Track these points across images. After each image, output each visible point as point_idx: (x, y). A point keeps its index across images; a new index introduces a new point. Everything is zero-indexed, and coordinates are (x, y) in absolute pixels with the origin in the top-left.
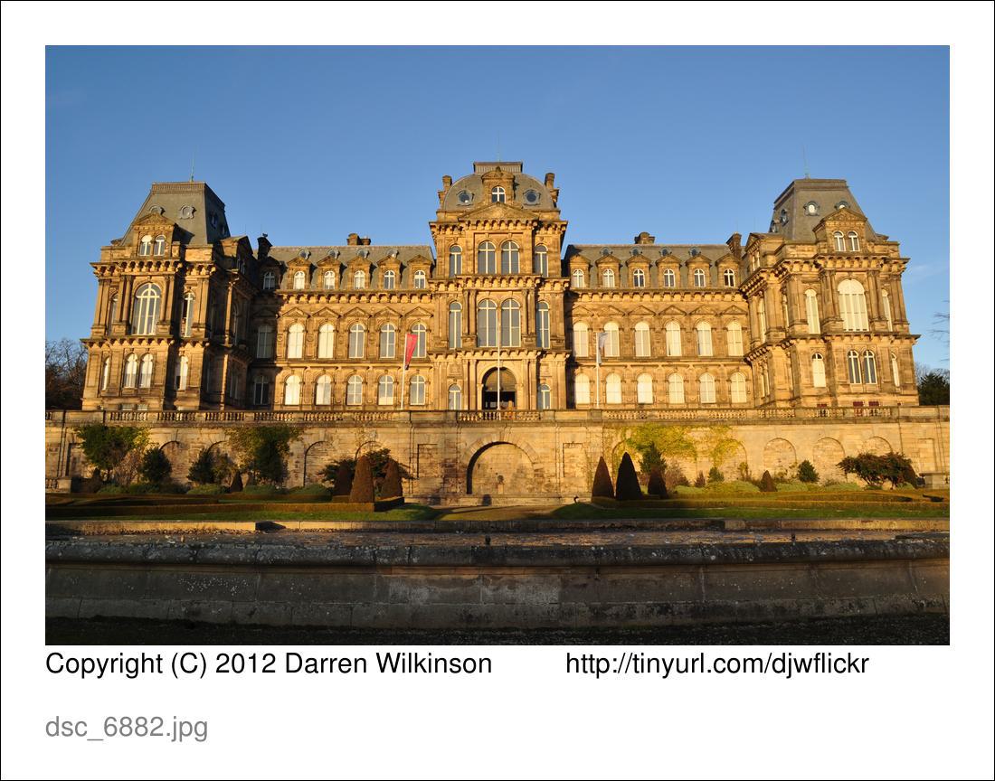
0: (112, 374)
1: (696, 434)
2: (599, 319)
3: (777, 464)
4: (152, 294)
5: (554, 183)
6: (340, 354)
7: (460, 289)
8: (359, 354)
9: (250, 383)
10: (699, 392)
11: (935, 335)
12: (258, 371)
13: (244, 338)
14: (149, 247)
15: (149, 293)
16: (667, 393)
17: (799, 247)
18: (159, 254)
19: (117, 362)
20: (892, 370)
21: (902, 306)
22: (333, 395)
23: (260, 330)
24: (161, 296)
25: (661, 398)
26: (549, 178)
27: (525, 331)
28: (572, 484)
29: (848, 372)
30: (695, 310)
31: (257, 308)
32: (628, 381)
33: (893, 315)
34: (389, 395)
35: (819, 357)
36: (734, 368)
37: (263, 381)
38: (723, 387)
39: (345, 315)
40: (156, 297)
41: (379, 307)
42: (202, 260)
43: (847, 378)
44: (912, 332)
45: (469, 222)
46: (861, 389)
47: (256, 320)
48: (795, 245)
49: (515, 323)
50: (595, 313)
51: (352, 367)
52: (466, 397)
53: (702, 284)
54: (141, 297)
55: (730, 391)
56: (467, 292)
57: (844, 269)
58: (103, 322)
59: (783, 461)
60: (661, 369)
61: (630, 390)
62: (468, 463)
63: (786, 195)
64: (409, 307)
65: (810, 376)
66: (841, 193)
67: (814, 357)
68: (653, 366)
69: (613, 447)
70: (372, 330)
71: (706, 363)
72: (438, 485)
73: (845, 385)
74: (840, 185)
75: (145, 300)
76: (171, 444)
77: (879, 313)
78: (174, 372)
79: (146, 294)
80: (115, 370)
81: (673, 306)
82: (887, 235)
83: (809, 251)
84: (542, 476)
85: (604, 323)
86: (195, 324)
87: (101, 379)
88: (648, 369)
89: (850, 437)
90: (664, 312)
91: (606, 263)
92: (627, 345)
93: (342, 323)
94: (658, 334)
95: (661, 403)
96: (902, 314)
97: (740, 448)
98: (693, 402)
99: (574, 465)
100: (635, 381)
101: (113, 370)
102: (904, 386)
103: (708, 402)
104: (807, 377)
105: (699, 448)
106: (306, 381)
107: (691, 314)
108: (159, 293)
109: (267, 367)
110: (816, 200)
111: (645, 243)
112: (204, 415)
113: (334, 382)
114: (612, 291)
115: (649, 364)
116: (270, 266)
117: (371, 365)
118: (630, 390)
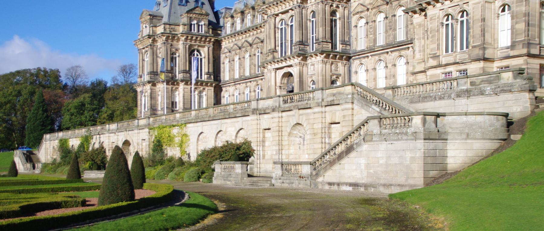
32: (390, 66)
51: (255, 81)
68: (405, 49)
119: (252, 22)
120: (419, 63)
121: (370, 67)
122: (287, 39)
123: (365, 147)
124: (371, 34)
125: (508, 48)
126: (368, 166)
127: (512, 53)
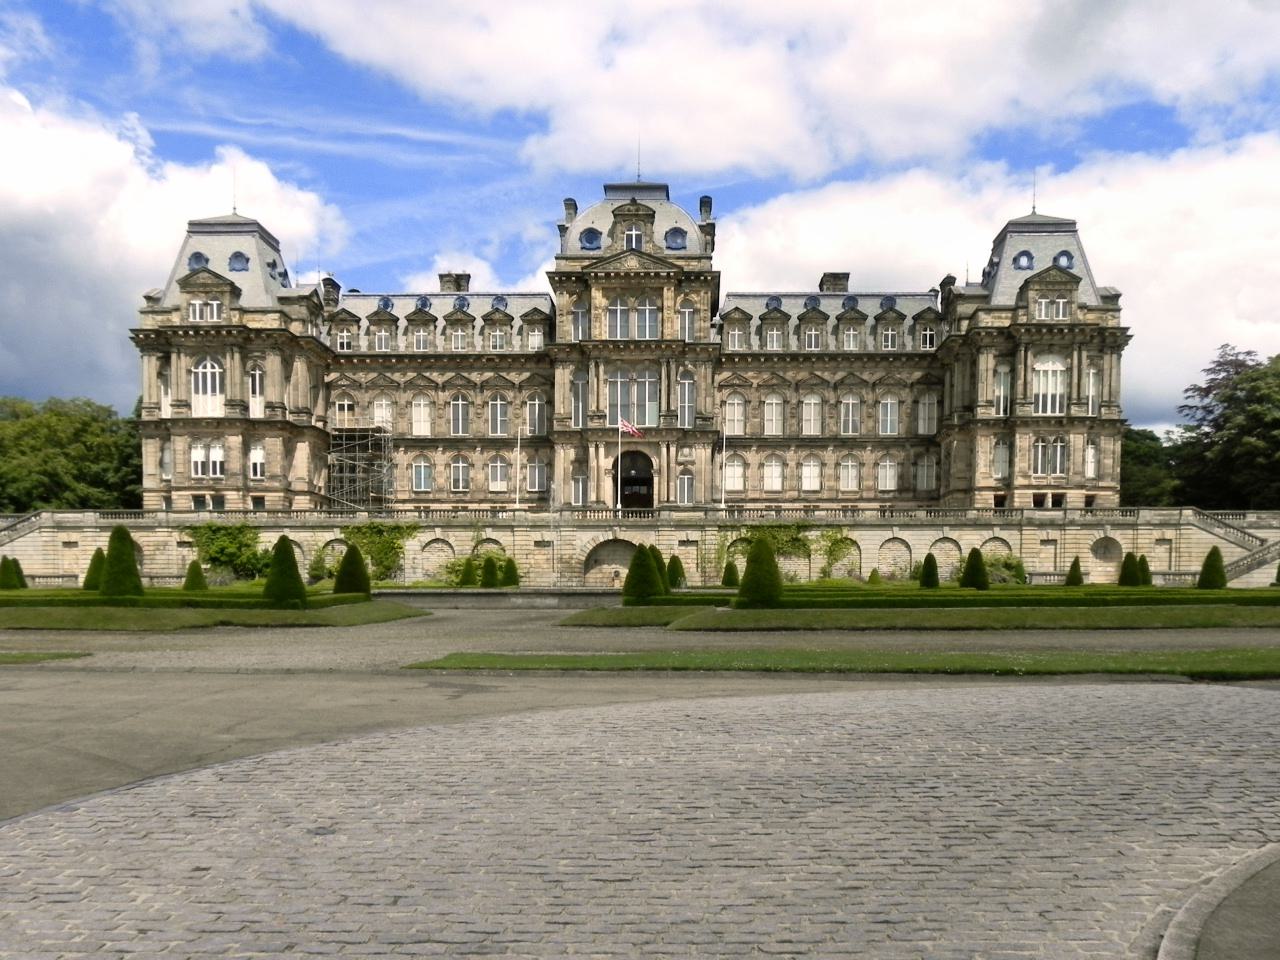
0: (178, 461)
1: (812, 532)
11: (1186, 411)
19: (181, 448)
29: (1032, 462)
43: (1029, 468)
45: (596, 274)
46: (1044, 482)
48: (989, 311)
57: (1044, 342)
61: (793, 478)
72: (555, 580)
78: (249, 459)
82: (1120, 289)
92: (794, 421)
99: (689, 561)
107: (874, 384)
122: (655, 405)
124: (755, 417)
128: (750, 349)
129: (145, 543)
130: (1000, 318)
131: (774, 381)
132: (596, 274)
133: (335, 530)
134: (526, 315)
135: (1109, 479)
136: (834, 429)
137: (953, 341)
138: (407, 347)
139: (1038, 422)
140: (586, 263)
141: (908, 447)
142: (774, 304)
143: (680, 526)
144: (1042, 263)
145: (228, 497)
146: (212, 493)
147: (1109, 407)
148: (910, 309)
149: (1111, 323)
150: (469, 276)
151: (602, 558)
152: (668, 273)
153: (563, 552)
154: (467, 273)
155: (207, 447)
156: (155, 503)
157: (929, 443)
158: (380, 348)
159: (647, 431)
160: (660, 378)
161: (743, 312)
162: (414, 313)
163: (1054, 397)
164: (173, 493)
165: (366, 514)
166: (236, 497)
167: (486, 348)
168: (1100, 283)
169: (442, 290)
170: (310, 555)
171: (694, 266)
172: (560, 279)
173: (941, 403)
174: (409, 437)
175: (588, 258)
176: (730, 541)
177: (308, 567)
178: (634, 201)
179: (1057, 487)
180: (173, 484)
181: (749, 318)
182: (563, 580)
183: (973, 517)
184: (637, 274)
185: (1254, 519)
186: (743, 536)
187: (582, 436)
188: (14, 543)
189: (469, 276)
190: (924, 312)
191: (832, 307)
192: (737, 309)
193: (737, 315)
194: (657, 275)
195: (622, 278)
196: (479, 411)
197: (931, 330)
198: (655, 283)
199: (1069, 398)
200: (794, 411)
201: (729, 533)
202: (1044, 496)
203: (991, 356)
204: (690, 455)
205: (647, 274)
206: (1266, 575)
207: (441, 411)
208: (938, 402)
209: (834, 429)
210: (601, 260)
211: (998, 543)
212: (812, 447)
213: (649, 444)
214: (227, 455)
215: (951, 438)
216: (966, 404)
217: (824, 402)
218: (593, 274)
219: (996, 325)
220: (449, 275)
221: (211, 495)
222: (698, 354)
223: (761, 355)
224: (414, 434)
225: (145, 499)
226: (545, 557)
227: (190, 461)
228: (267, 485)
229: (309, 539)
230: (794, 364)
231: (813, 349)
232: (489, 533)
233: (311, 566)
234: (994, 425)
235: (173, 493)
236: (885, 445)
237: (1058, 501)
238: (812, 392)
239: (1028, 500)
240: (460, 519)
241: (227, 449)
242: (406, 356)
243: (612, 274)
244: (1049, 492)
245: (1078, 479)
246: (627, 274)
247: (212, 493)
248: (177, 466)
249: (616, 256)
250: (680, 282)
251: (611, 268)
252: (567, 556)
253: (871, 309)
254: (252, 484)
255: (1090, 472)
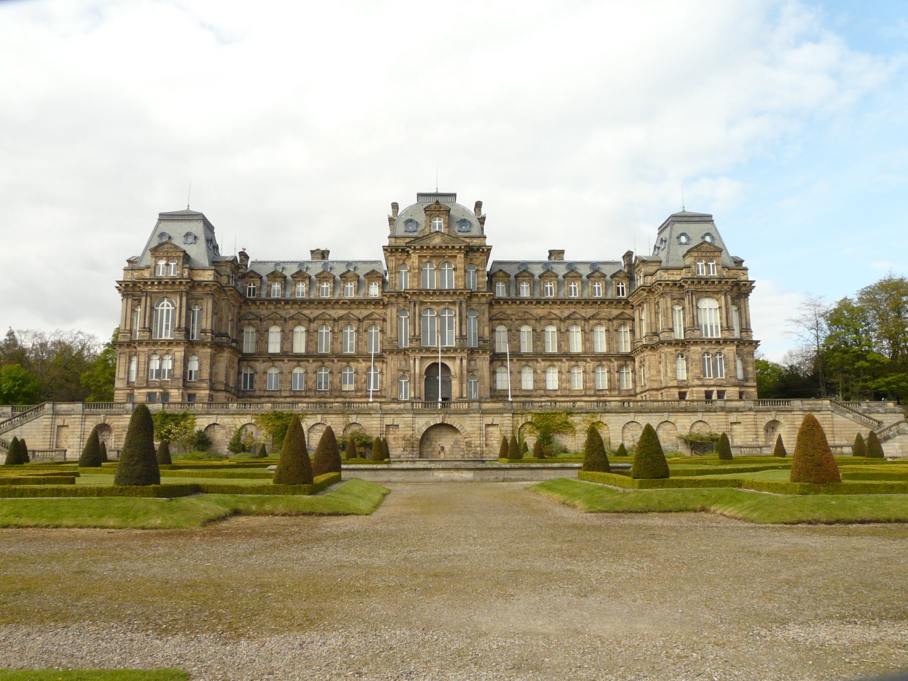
1: (576, 418)
2: (517, 322)
3: (631, 439)
4: (168, 306)
5: (482, 209)
6: (311, 349)
7: (407, 300)
8: (326, 349)
9: (239, 373)
10: (594, 381)
12: (245, 363)
13: (234, 338)
14: (163, 268)
15: (165, 305)
16: (569, 381)
17: (670, 272)
18: (172, 275)
20: (736, 368)
21: (748, 317)
22: (306, 382)
23: (246, 330)
24: (176, 308)
25: (564, 385)
26: (478, 205)
27: (458, 334)
28: (490, 452)
30: (593, 316)
31: (242, 312)
32: (539, 371)
33: (741, 325)
34: (351, 383)
35: (682, 357)
36: (622, 362)
37: (249, 372)
38: (614, 377)
39: (315, 319)
40: (171, 308)
41: (342, 312)
42: (206, 279)
44: (754, 338)
45: (415, 247)
47: (242, 322)
49: (450, 327)
50: (514, 317)
52: (412, 385)
53: (599, 294)
54: (160, 308)
55: (619, 380)
56: (413, 303)
58: (128, 328)
59: (635, 437)
60: (566, 364)
62: (420, 438)
63: (665, 225)
64: (365, 313)
65: (675, 371)
66: (705, 228)
67: (678, 357)
69: (519, 426)
70: (336, 330)
71: (600, 359)
72: (400, 453)
73: (699, 379)
74: (706, 219)
75: (162, 311)
76: (212, 427)
77: (727, 323)
78: (187, 367)
79: (163, 306)
80: (142, 367)
81: (575, 312)
82: (742, 258)
83: (677, 274)
84: (471, 447)
85: (521, 325)
86: (202, 330)
87: (128, 372)
88: (555, 363)
89: (681, 420)
90: (568, 317)
91: (523, 277)
92: (539, 343)
93: (312, 325)
94: (563, 335)
95: (565, 389)
96: (748, 323)
97: (606, 427)
98: (590, 389)
100: (544, 372)
101: (140, 366)
102: (746, 379)
103: (601, 388)
104: (671, 372)
105: (577, 428)
106: (284, 371)
107: (589, 319)
108: (173, 305)
109: (253, 360)
110: (687, 233)
111: (555, 258)
112: (236, 405)
113: (306, 372)
114: (527, 300)
115: (556, 358)
116: (252, 277)
117: (336, 360)
118: (540, 381)
119: (308, 293)
120: (671, 380)
121: (515, 370)
123: (898, 437)
125: (742, 380)
126: (901, 447)
127: (747, 384)
128: (509, 296)
129: (116, 426)
130: (673, 274)
131: (526, 317)
132: (415, 247)
133: (248, 416)
134: (367, 274)
135: (752, 381)
136: (566, 348)
137: (642, 289)
138: (291, 295)
139: (704, 342)
140: (408, 240)
141: (613, 360)
142: (523, 268)
143: (485, 412)
144: (696, 242)
145: (172, 394)
146: (161, 391)
147: (747, 332)
148: (609, 271)
149: (743, 278)
150: (328, 252)
151: (431, 437)
152: (460, 247)
153: (406, 433)
154: (328, 249)
155: (161, 359)
156: (122, 398)
157: (628, 358)
158: (274, 295)
159: (448, 350)
160: (455, 315)
161: (505, 273)
162: (297, 273)
163: (711, 327)
164: (135, 391)
165: (270, 405)
166: (177, 394)
167: (342, 295)
168: (732, 254)
169: (313, 258)
170: (231, 434)
171: (476, 242)
172: (392, 250)
173: (632, 331)
174: (291, 354)
175: (409, 237)
176: (521, 424)
177: (228, 443)
178: (437, 202)
179: (720, 386)
180: (136, 385)
181: (509, 276)
182: (405, 453)
183: (683, 406)
184: (441, 247)
185: (866, 408)
186: (529, 420)
187: (405, 353)
188: (24, 427)
189: (328, 252)
190: (617, 273)
191: (561, 271)
192: (501, 270)
193: (501, 274)
194: (453, 247)
195: (431, 249)
196: (336, 337)
197: (622, 284)
198: (454, 253)
199: (722, 327)
200: (539, 337)
201: (520, 419)
202: (712, 392)
203: (669, 300)
204: (475, 365)
205: (447, 247)
206: (890, 448)
207: (311, 337)
208: (630, 331)
209: (566, 348)
210: (417, 238)
211: (702, 424)
212: (552, 361)
213: (449, 358)
214: (173, 365)
215: (645, 354)
216: (653, 331)
217: (559, 330)
218: (413, 247)
219: (671, 279)
220: (318, 250)
221: (160, 392)
222: (479, 298)
223: (509, 300)
224: (294, 352)
225: (115, 395)
226: (393, 436)
227: (148, 369)
228: (198, 385)
229: (230, 423)
230: (539, 305)
231: (549, 296)
232: (353, 419)
233: (231, 444)
234: (675, 344)
235: (135, 391)
236: (600, 359)
237: (721, 395)
238: (551, 324)
239: (702, 395)
240: (334, 408)
241: (174, 361)
242: (290, 300)
243: (425, 247)
244: (715, 389)
245: (733, 380)
246: (434, 247)
247: (161, 391)
248: (140, 372)
249: (427, 235)
250: (467, 252)
251: (425, 244)
252: (409, 436)
253: (585, 271)
254: (188, 384)
255: (740, 375)
